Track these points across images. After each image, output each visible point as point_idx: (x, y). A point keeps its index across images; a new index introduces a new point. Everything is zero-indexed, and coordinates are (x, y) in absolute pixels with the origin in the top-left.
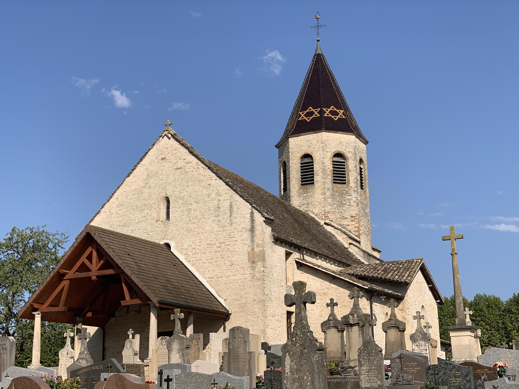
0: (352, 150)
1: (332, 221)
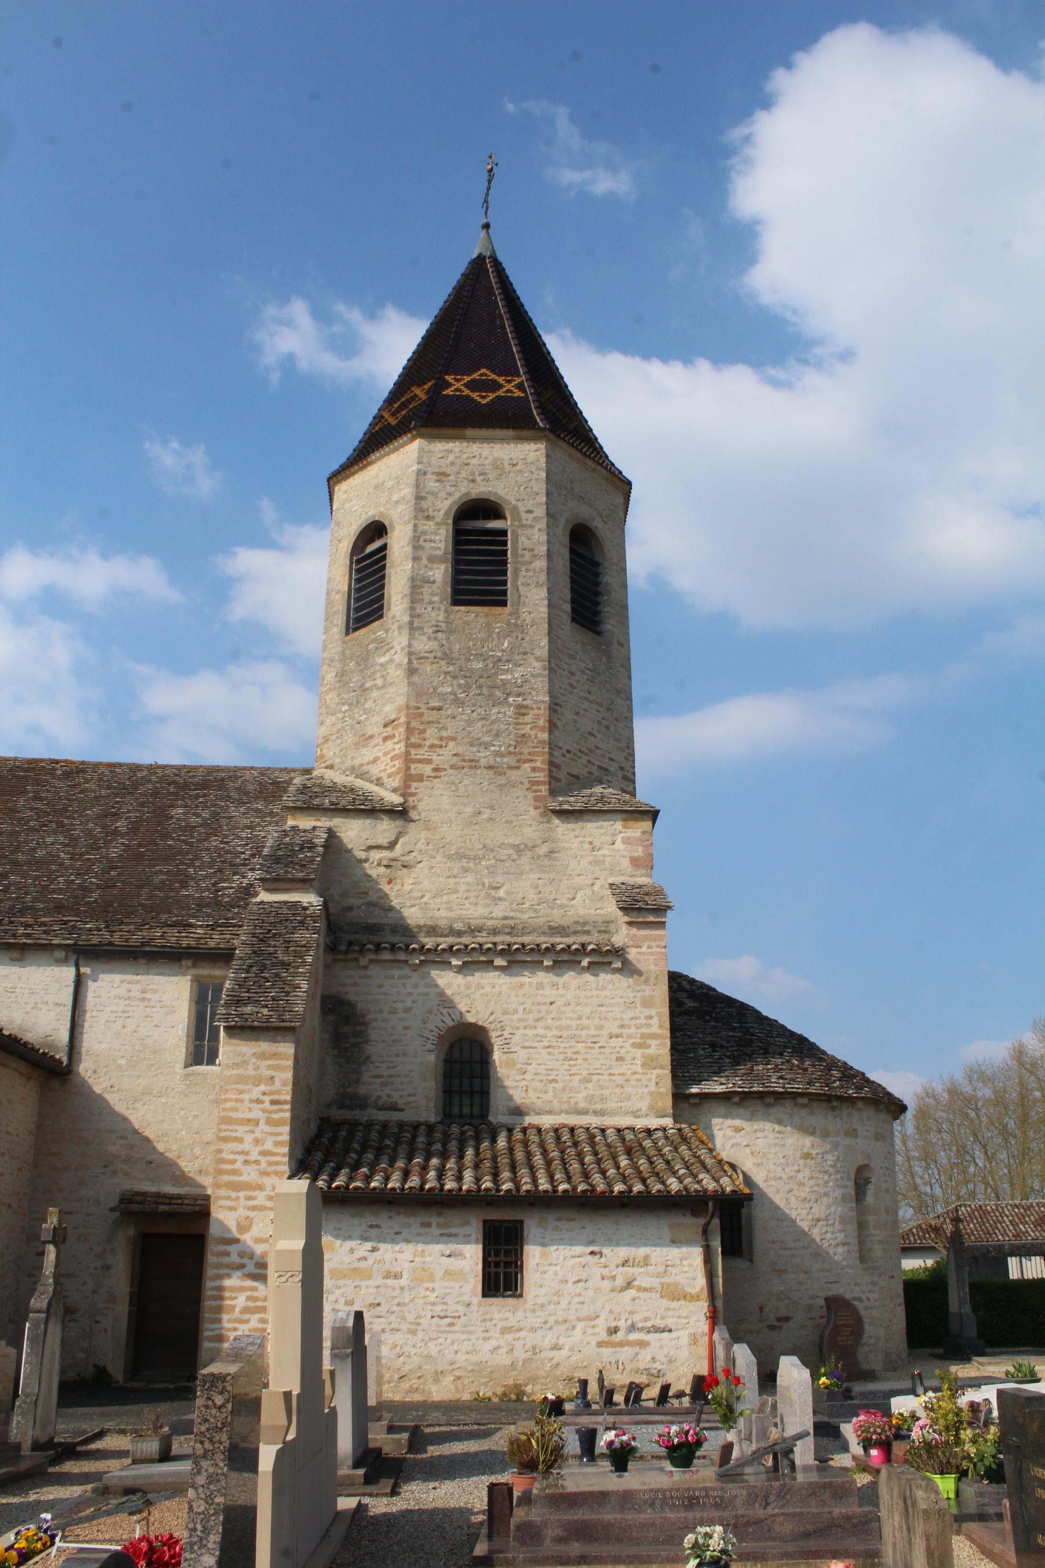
0: (407, 492)
1: (331, 767)
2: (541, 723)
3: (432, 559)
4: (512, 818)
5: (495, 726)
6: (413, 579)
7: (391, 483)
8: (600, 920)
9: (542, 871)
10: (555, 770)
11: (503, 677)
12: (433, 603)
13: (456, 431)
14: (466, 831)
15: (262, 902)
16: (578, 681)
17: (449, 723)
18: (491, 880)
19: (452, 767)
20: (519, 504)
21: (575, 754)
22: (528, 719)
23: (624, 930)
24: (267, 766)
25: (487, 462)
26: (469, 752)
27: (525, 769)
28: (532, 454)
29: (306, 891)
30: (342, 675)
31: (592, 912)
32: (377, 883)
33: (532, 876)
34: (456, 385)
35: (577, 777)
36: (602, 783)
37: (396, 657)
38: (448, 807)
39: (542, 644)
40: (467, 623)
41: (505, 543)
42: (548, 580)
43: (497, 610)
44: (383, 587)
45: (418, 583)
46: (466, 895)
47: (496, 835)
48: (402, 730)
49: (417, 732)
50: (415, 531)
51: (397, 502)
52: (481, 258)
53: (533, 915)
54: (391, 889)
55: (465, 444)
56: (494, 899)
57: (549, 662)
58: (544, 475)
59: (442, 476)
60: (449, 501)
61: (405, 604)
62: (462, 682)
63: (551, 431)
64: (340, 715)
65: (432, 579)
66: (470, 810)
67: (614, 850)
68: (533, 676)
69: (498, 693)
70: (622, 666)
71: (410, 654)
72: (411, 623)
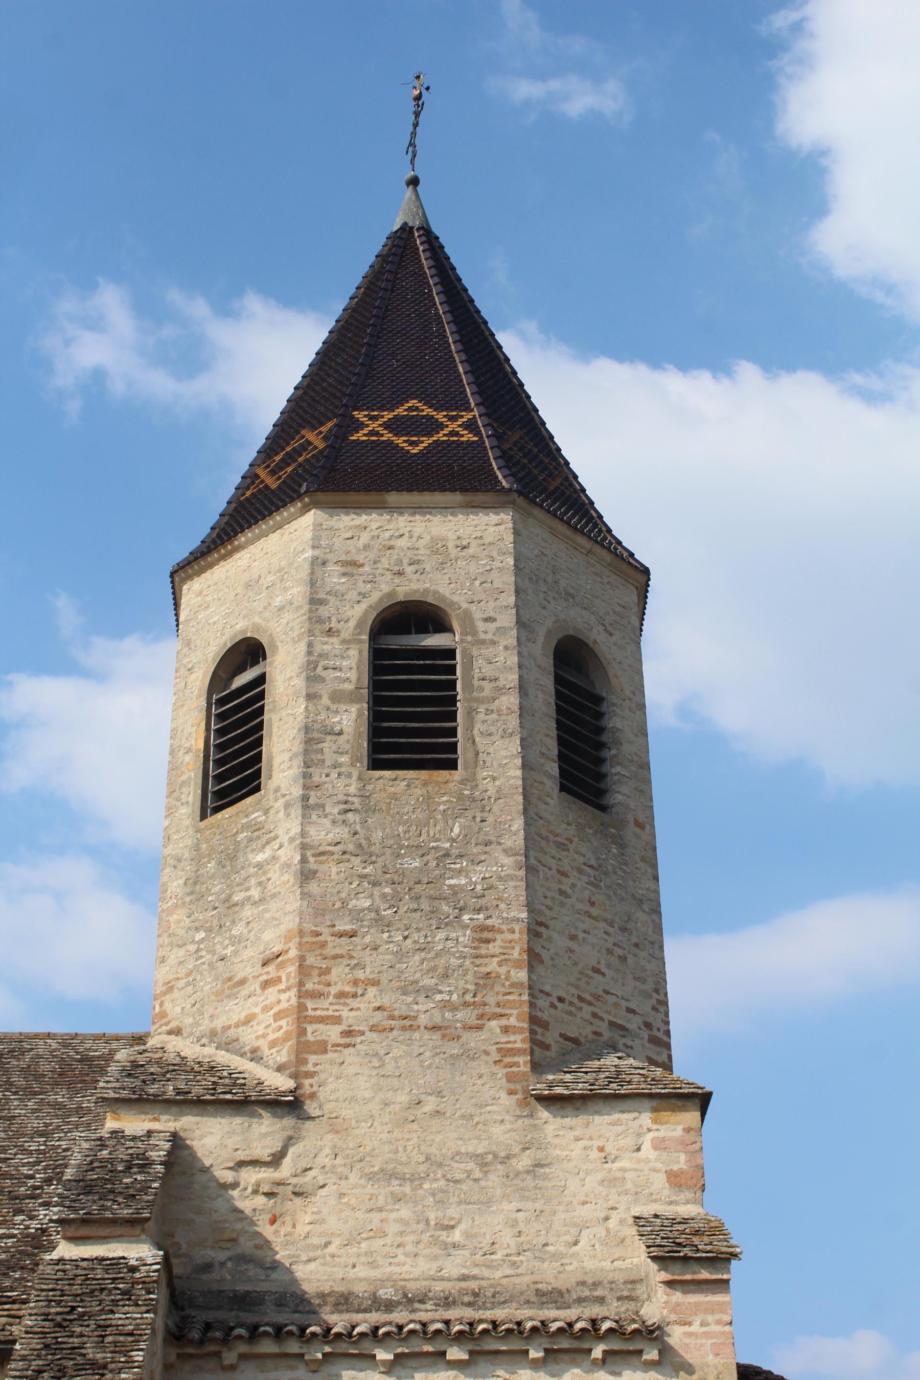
0: (297, 592)
1: (177, 1032)
2: (516, 954)
3: (337, 697)
4: (471, 1110)
5: (442, 962)
6: (307, 729)
7: (270, 578)
8: (620, 1277)
9: (523, 1198)
10: (539, 1030)
11: (453, 882)
12: (340, 765)
13: (373, 497)
14: (397, 1134)
15: (61, 1261)
16: (573, 885)
17: (367, 957)
18: (440, 1214)
19: (373, 1029)
20: (473, 608)
21: (571, 1003)
22: (494, 948)
23: (661, 1294)
24: (72, 1031)
25: (421, 543)
26: (401, 1004)
27: (491, 1030)
28: (492, 529)
29: (134, 1239)
30: (196, 883)
31: (607, 1264)
32: (253, 1223)
33: (506, 1206)
34: (371, 426)
35: (575, 1041)
36: (616, 1050)
37: (280, 852)
38: (368, 1094)
39: (514, 828)
40: (395, 797)
41: (452, 670)
42: (521, 726)
43: (442, 775)
44: (259, 742)
45: (316, 735)
46: (399, 1240)
47: (448, 1138)
48: (292, 969)
49: (317, 971)
50: (309, 653)
51: (281, 609)
52: (406, 229)
53: (509, 1272)
54: (276, 1232)
55: (387, 517)
56: (445, 1246)
57: (526, 856)
58: (511, 561)
59: (350, 566)
60: (363, 606)
61: (296, 769)
62: (388, 890)
63: (520, 493)
64: (192, 948)
65: (337, 728)
66: (403, 1098)
67: (639, 1161)
68: (500, 878)
69: (445, 908)
70: (643, 859)
71: (304, 847)
72: (305, 798)
